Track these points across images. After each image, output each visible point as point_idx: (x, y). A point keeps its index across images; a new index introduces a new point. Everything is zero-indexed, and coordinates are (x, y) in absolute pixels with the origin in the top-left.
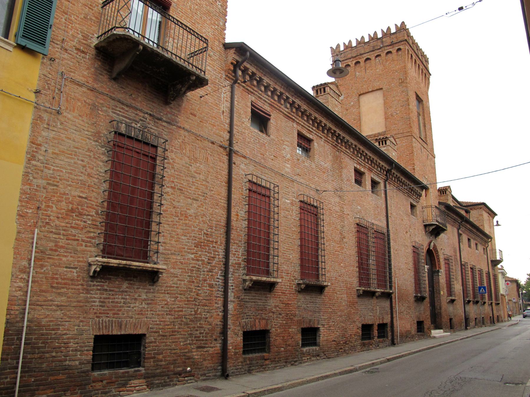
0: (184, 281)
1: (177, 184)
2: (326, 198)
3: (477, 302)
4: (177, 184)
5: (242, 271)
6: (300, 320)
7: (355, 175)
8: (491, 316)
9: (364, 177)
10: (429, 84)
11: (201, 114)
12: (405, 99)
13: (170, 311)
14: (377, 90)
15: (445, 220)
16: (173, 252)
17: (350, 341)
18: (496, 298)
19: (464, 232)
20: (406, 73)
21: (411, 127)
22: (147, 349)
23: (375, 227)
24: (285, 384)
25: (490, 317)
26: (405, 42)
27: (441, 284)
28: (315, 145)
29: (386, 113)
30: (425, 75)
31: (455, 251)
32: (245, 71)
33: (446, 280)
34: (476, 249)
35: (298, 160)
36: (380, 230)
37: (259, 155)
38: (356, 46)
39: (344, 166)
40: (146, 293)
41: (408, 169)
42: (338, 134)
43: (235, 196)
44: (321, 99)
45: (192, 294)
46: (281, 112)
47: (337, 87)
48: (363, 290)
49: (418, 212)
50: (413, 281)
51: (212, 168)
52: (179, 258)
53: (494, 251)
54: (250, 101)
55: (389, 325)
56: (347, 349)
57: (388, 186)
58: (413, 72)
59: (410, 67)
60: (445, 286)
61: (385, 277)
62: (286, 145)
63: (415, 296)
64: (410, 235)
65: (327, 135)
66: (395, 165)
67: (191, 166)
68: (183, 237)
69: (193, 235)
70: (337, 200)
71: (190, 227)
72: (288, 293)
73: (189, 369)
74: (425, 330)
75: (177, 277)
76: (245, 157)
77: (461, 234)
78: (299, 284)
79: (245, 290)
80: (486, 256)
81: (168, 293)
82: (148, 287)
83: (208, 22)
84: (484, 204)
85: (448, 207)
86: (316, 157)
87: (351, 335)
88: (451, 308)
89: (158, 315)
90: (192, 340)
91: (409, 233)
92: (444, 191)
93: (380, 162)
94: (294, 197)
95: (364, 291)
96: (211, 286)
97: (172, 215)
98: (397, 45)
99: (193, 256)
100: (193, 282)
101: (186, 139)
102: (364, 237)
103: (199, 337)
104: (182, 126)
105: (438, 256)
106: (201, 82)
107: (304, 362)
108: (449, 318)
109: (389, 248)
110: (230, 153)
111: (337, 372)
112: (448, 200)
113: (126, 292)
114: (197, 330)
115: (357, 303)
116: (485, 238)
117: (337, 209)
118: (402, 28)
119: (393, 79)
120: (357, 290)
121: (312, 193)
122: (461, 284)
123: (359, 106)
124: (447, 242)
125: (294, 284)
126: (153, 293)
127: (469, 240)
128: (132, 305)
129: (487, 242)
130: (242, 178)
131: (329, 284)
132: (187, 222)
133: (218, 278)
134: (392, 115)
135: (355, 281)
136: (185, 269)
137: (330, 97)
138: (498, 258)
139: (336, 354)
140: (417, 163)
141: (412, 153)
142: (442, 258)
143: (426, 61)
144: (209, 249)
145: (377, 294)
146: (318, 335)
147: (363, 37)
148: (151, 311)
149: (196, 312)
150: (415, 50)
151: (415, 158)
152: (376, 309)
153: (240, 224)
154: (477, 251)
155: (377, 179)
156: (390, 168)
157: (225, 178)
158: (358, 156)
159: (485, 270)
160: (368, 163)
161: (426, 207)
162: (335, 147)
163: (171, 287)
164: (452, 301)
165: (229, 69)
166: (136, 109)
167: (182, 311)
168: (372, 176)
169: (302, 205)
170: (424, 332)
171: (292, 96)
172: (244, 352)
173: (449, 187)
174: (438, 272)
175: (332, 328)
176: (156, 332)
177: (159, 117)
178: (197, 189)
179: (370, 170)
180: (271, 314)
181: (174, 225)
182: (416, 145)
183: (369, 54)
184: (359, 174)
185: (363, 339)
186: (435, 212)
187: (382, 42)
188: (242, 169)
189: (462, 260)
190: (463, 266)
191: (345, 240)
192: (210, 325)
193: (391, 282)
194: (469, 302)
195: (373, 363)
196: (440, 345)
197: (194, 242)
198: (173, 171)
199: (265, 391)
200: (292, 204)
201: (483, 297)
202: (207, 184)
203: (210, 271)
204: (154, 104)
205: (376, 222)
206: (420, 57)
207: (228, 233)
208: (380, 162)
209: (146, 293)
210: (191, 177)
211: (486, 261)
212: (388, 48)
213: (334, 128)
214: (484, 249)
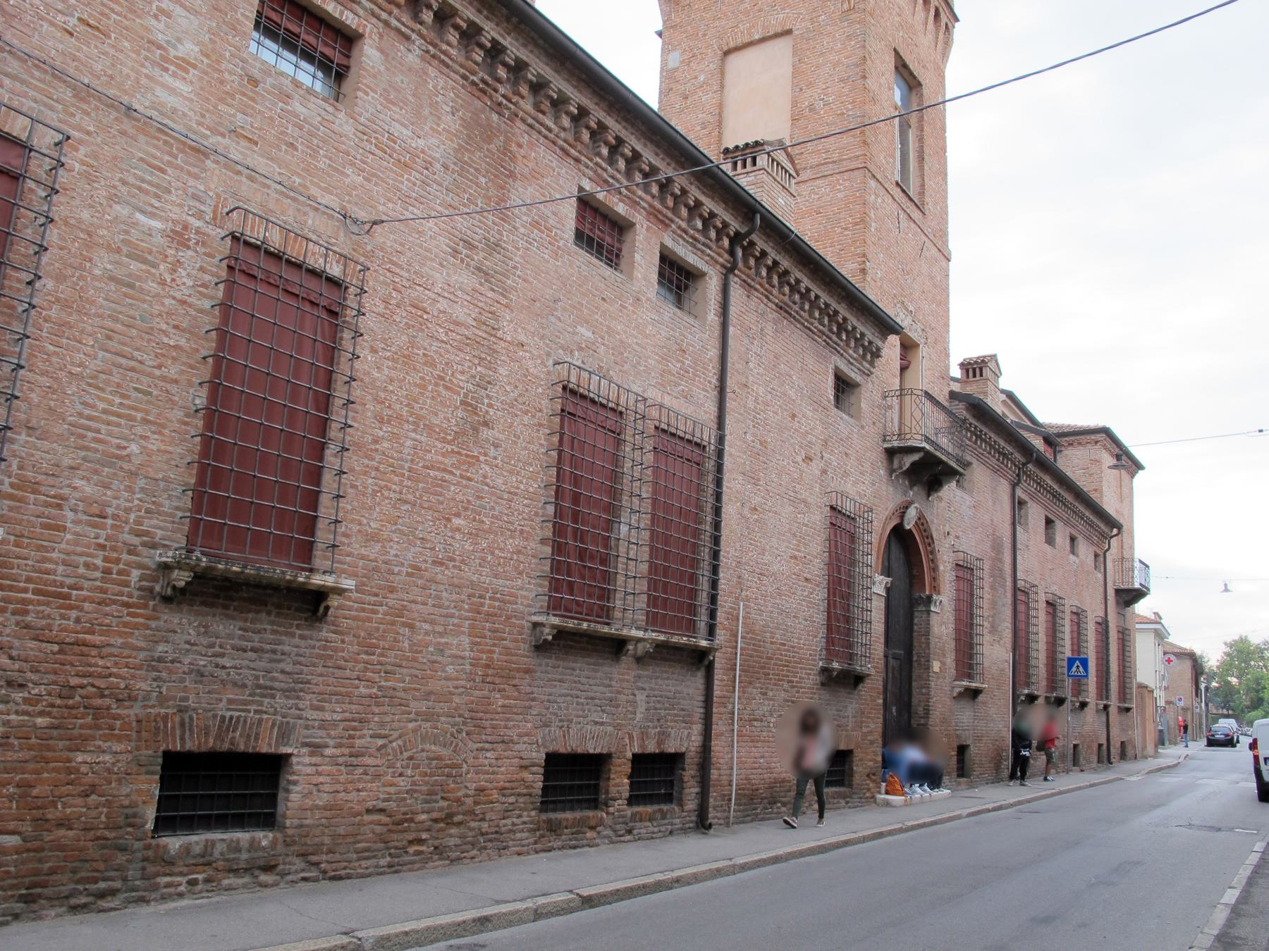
2: (402, 260)
3: (1060, 702)
7: (580, 218)
8: (1104, 741)
9: (628, 237)
10: (948, 43)
12: (854, 59)
14: (777, 36)
15: (961, 446)
17: (472, 813)
18: (1121, 693)
21: (865, 142)
23: (654, 413)
25: (1100, 746)
27: (933, 641)
28: (369, 54)
29: (795, 103)
30: (937, 14)
31: (997, 546)
33: (957, 630)
34: (1073, 552)
36: (682, 428)
41: (847, 269)
48: (553, 627)
49: (863, 405)
50: (820, 618)
53: (1125, 561)
56: (452, 842)
57: (736, 292)
60: (951, 645)
61: (693, 594)
63: (825, 671)
64: (824, 472)
66: (763, 218)
70: (466, 279)
72: (85, 599)
74: (857, 779)
77: (1022, 503)
80: (1100, 576)
84: (1106, 431)
85: (980, 410)
87: (481, 790)
88: (965, 715)
91: (816, 467)
93: (702, 198)
94: (199, 215)
95: (561, 634)
105: (932, 553)
107: (164, 898)
108: (955, 745)
115: (527, 671)
116: (1104, 525)
120: (536, 625)
122: (1009, 645)
123: (722, 86)
124: (968, 517)
125: (139, 566)
127: (1049, 522)
129: (1105, 537)
131: (348, 583)
134: (811, 108)
138: (1137, 586)
139: (383, 862)
141: (863, 221)
146: (283, 783)
152: (634, 703)
154: (1071, 556)
156: (743, 230)
158: (599, 154)
159: (1094, 612)
162: (482, 90)
168: (669, 243)
170: (850, 786)
173: (994, 357)
175: (367, 760)
185: (545, 806)
189: (1020, 575)
190: (1020, 596)
191: (485, 433)
196: (880, 835)
200: (179, 237)
201: (1078, 687)
211: (1102, 589)
214: (1096, 556)
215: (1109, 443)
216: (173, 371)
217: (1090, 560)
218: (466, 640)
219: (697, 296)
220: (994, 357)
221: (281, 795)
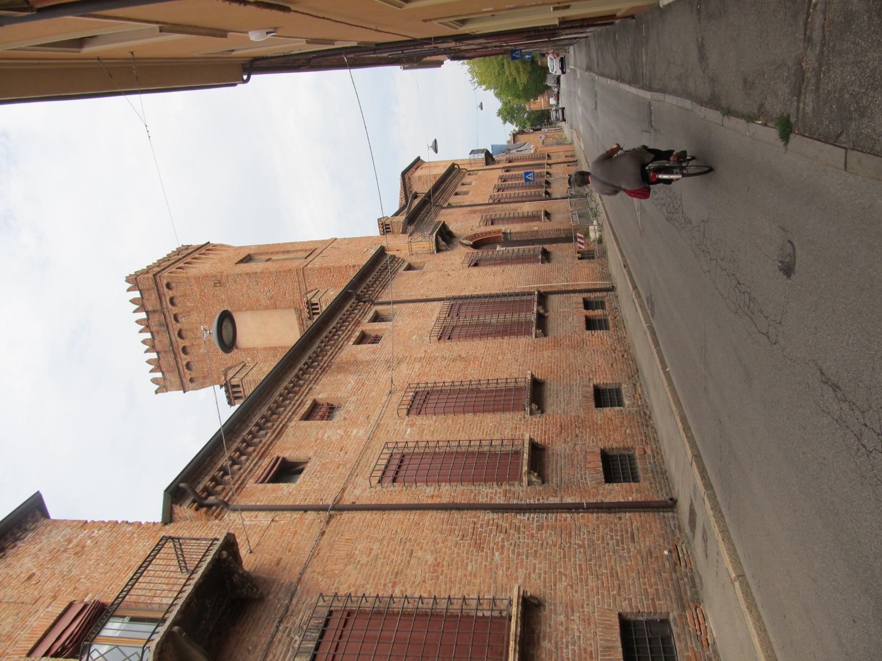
0: (535, 564)
1: (388, 580)
2: (402, 381)
3: (547, 183)
4: (388, 580)
5: (516, 487)
6: (584, 409)
9: (368, 332)
10: (222, 246)
11: (277, 551)
12: (247, 279)
13: (581, 581)
16: (492, 581)
19: (446, 201)
20: (206, 277)
22: (641, 610)
24: (676, 413)
26: (158, 277)
29: (267, 308)
31: (475, 212)
32: (209, 492)
35: (345, 419)
37: (339, 471)
38: (158, 353)
39: (352, 359)
40: (556, 614)
41: (353, 274)
42: (304, 364)
43: (404, 501)
44: (249, 390)
45: (554, 552)
46: (271, 443)
47: (230, 368)
50: (520, 266)
51: (361, 532)
52: (501, 573)
53: (470, 163)
54: (255, 485)
55: (586, 295)
57: (380, 300)
58: (204, 267)
59: (197, 270)
60: (525, 224)
62: (323, 436)
63: (542, 262)
65: (306, 381)
67: (359, 561)
68: (469, 568)
69: (465, 555)
70: (403, 366)
71: (453, 560)
73: (666, 552)
75: (530, 574)
76: (344, 490)
77: (449, 204)
78: (532, 413)
79: (543, 482)
81: (555, 585)
82: (547, 612)
83: (127, 547)
84: (404, 174)
86: (339, 394)
88: (557, 217)
89: (588, 597)
90: (623, 549)
91: (451, 273)
92: (385, 227)
95: (538, 327)
96: (540, 528)
97: (435, 584)
98: (161, 289)
99: (497, 554)
100: (536, 552)
101: (318, 570)
102: (457, 331)
103: (617, 540)
104: (298, 576)
106: (230, 544)
109: (472, 297)
110: (338, 508)
111: (654, 351)
112: (398, 222)
113: (556, 643)
114: (608, 544)
116: (453, 171)
117: (417, 366)
118: (135, 281)
119: (214, 296)
120: (536, 337)
121: (396, 399)
122: (522, 204)
126: (555, 605)
127: (456, 194)
128: (577, 633)
130: (376, 492)
131: (529, 372)
132: (445, 563)
133: (528, 519)
135: (523, 341)
136: (517, 564)
137: (247, 378)
138: (483, 156)
140: (345, 262)
141: (329, 269)
142: (484, 229)
143: (187, 249)
144: (485, 532)
145: (542, 311)
147: (144, 342)
148: (583, 607)
149: (580, 546)
150: (169, 263)
151: (337, 265)
153: (447, 493)
155: (371, 314)
156: (355, 297)
157: (376, 516)
160: (347, 327)
161: (411, 250)
162: (324, 370)
163: (545, 581)
164: (547, 214)
165: (206, 513)
166: (271, 643)
167: (580, 566)
169: (413, 411)
171: (247, 426)
172: (635, 479)
174: (504, 233)
175: (593, 369)
176: (615, 599)
177: (282, 610)
178: (394, 552)
179: (358, 323)
180: (578, 448)
181: (450, 581)
182: (317, 263)
183: (171, 333)
184: (363, 339)
186: (417, 237)
187: (154, 311)
188: (362, 491)
189: (487, 202)
191: (464, 355)
192: (598, 527)
193: (523, 294)
194: (547, 193)
195: (640, 306)
197: (475, 554)
198: (368, 586)
199: (687, 437)
200: (412, 425)
201: (541, 175)
202: (387, 538)
203: (518, 529)
204: (263, 618)
205: (436, 315)
206: (180, 257)
207: (460, 508)
208: (346, 309)
209: (556, 614)
210: (376, 560)
212: (164, 303)
213: (296, 371)
215: (409, 173)
216: (462, 421)
217: (473, 177)
218: (545, 352)
219: (386, 313)
220: (379, 220)
221: (609, 387)
